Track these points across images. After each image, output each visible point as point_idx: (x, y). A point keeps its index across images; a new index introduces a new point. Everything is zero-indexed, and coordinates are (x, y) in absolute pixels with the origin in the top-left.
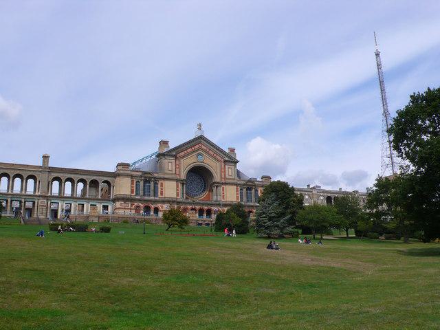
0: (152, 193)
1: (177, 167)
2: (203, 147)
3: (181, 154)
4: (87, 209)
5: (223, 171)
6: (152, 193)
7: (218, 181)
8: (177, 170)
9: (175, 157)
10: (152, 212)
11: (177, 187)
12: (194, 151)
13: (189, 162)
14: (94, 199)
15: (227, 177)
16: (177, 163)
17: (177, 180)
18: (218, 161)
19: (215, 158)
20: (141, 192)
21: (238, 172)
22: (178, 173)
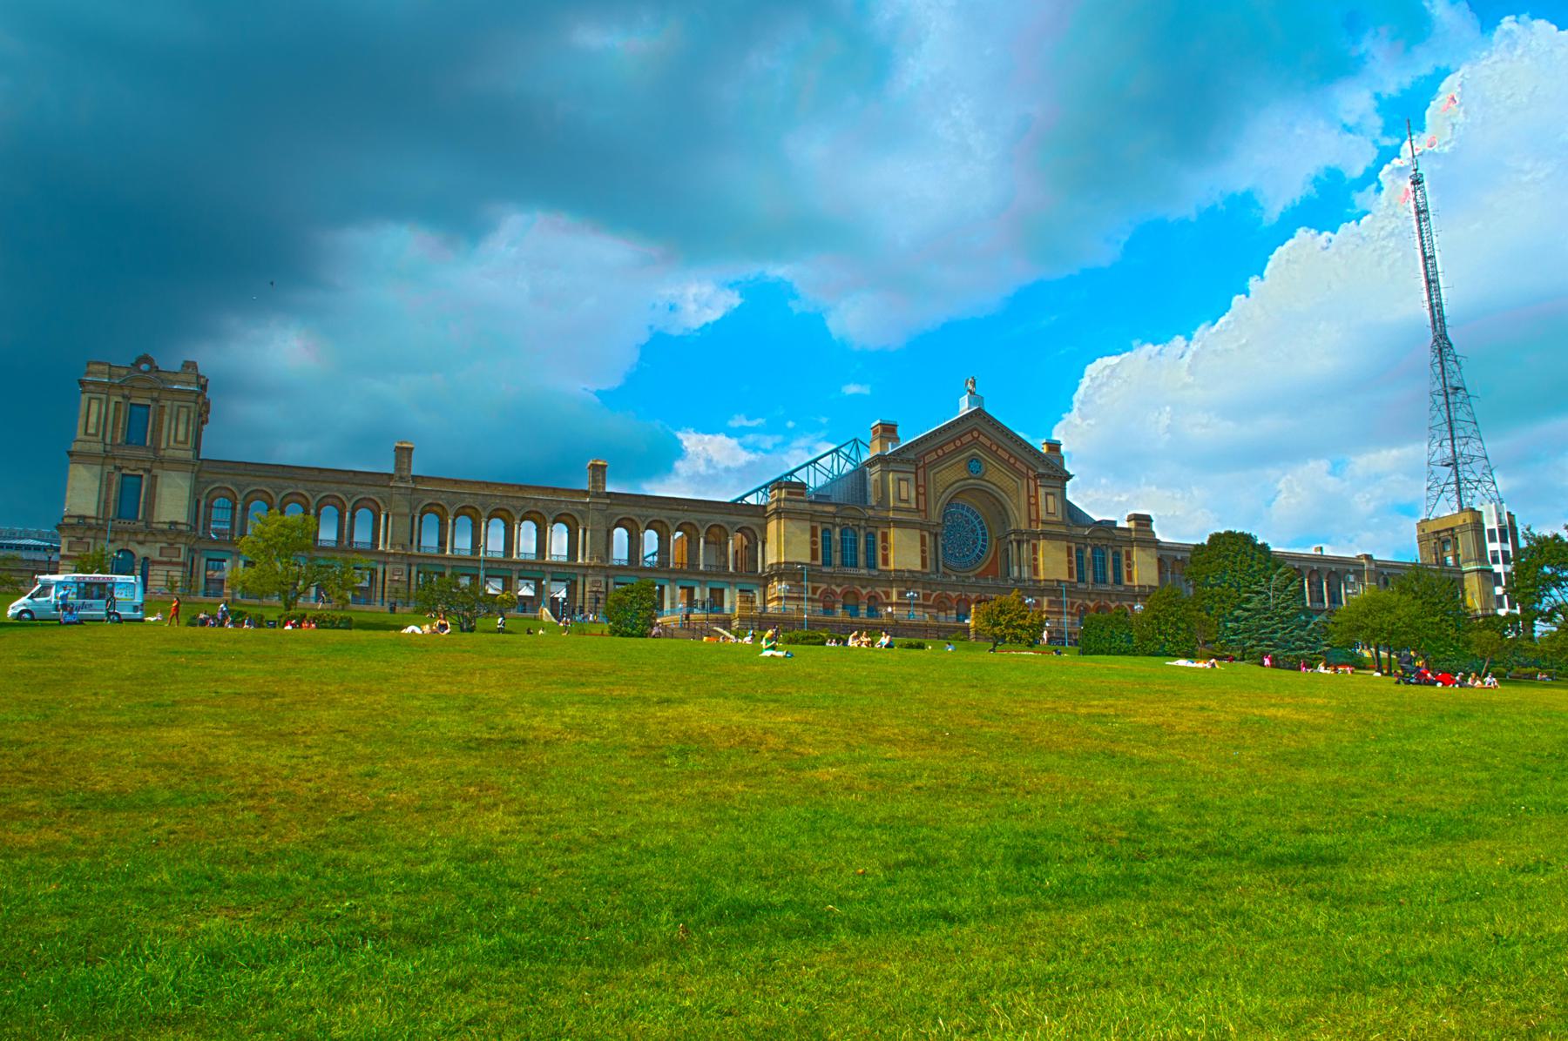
0: (862, 559)
1: (922, 490)
2: (982, 438)
3: (928, 459)
4: (733, 604)
5: (1032, 503)
6: (862, 559)
8: (922, 498)
9: (915, 462)
10: (863, 610)
11: (923, 543)
12: (958, 450)
13: (950, 475)
14: (718, 575)
15: (1043, 515)
16: (921, 482)
17: (920, 526)
18: (1020, 475)
19: (1013, 468)
20: (1089, 577)
21: (1070, 510)
22: (922, 507)
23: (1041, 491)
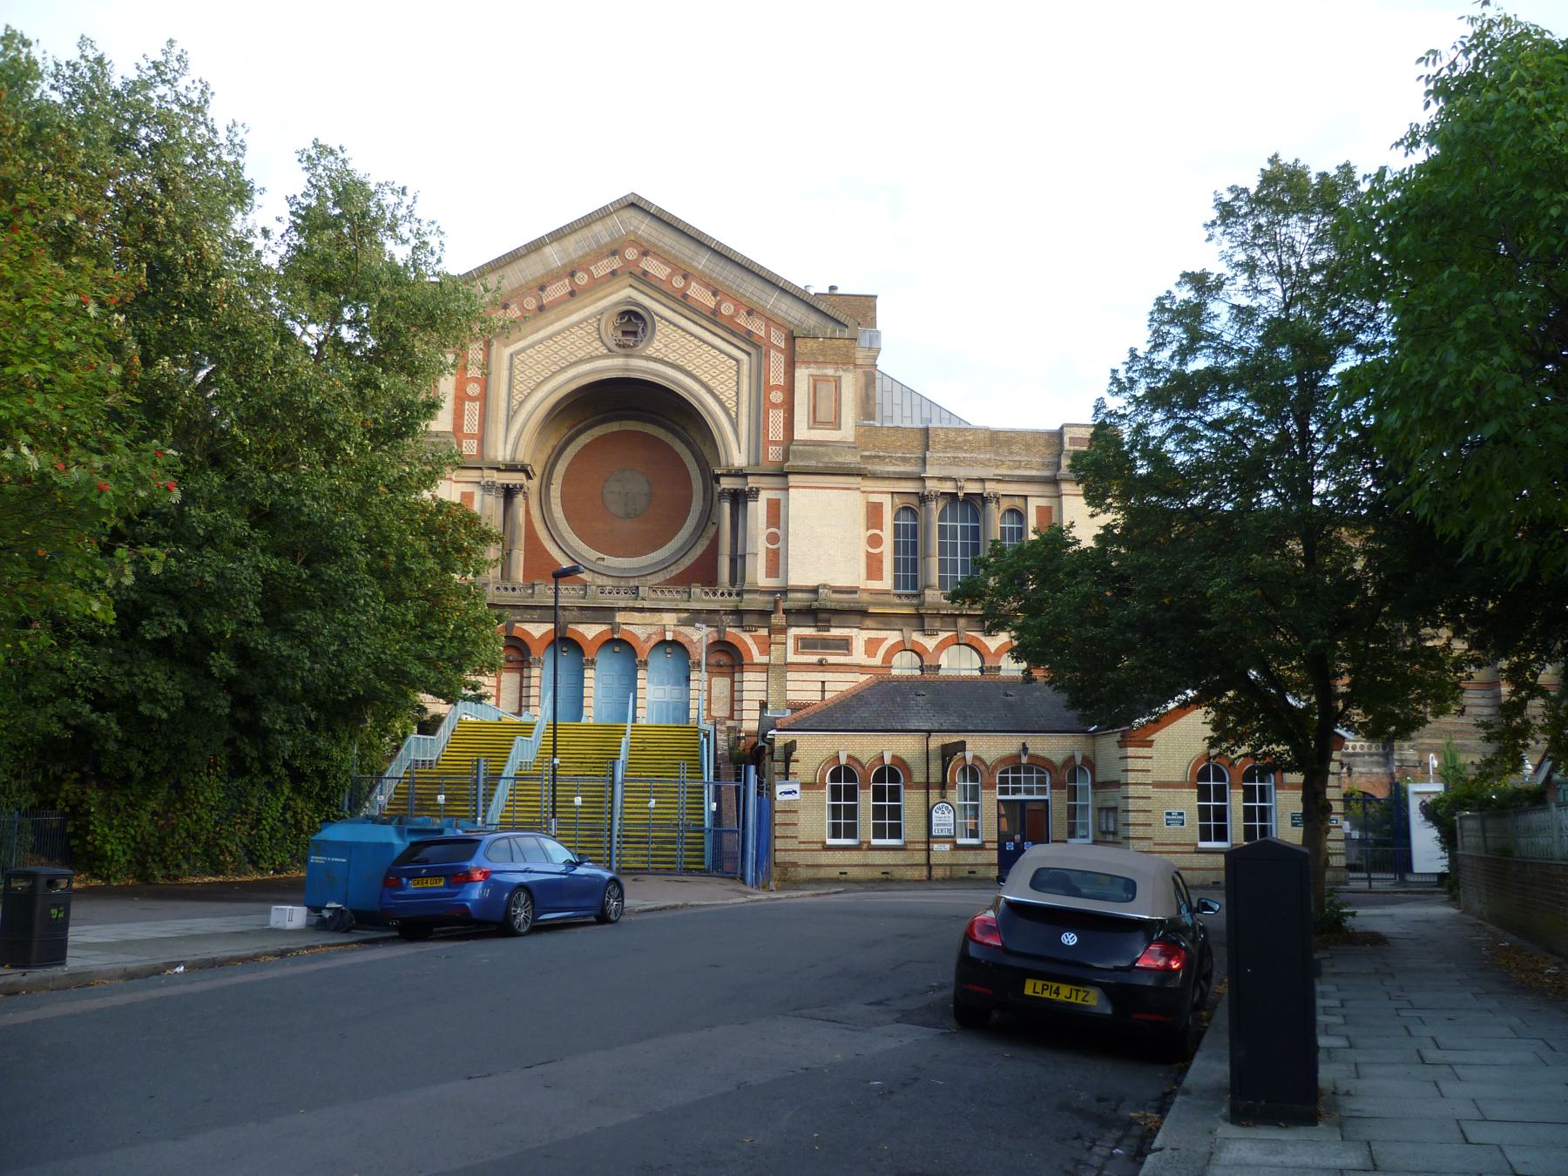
7: (738, 457)
23: (802, 375)
